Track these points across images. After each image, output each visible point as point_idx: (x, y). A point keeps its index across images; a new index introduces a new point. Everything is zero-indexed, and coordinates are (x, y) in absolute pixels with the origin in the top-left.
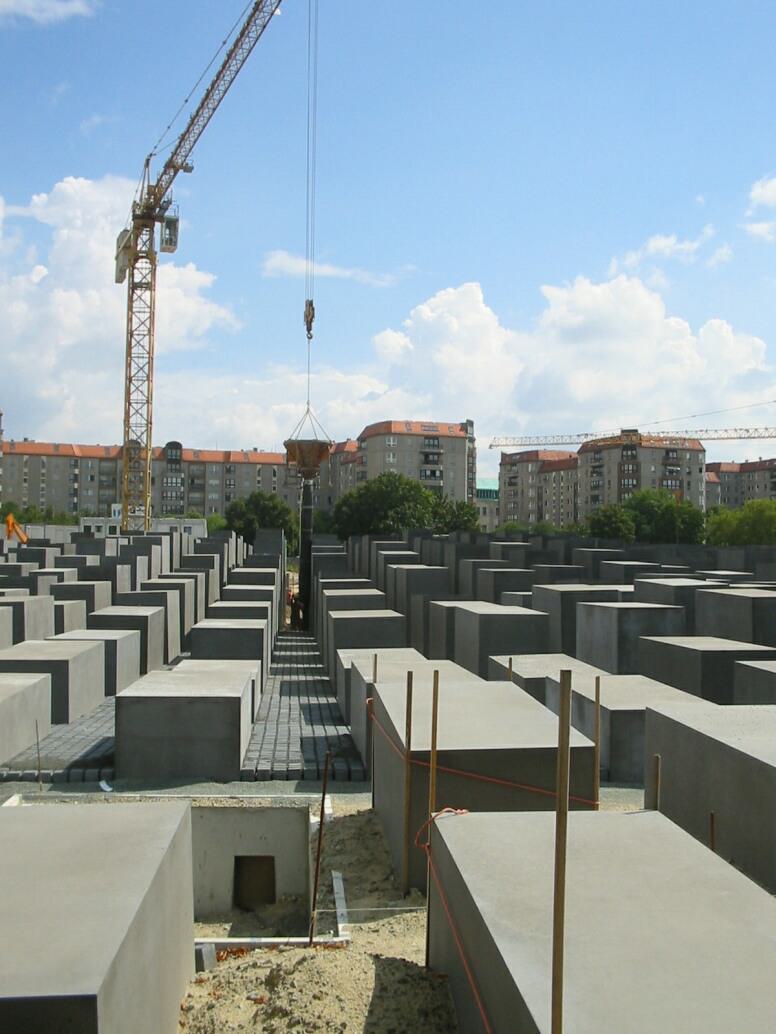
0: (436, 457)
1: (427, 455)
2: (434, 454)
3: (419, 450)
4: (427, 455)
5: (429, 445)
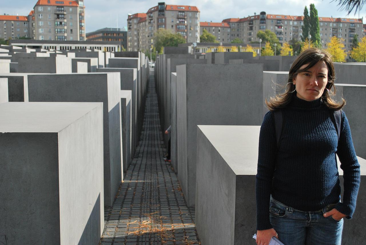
0: (63, 16)
1: (58, 15)
2: (62, 14)
3: (54, 13)
4: (58, 15)
5: (59, 10)
